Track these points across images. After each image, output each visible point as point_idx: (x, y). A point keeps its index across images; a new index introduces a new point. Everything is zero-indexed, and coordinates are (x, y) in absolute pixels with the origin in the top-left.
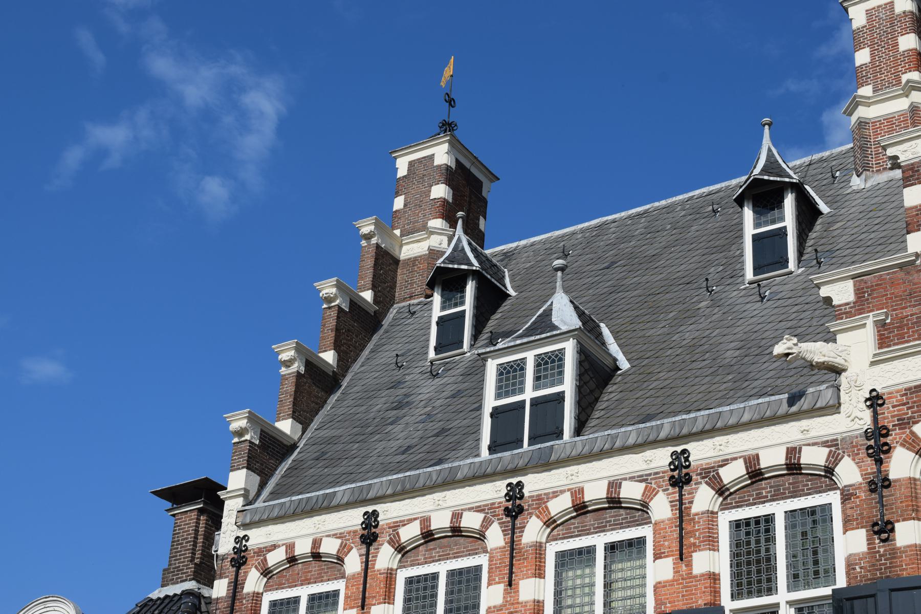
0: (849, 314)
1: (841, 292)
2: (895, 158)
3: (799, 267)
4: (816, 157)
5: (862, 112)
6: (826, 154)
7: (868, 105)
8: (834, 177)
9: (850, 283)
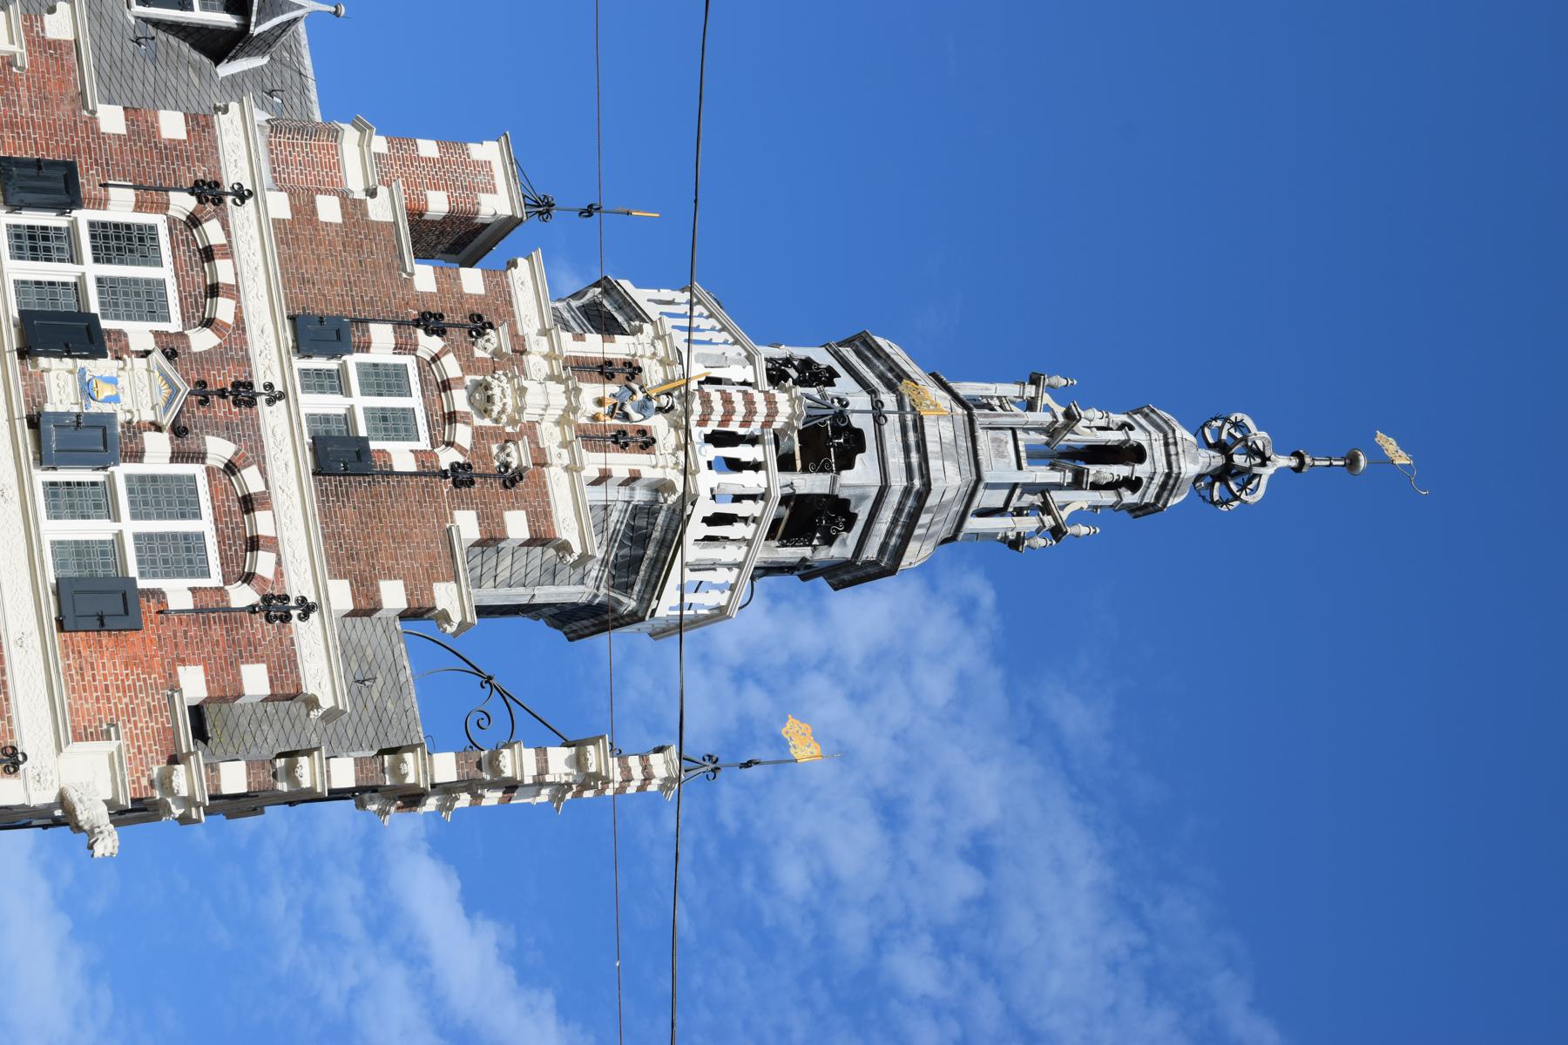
0: (28, 30)
1: (59, 26)
2: (226, 110)
3: (137, 17)
4: (312, 84)
5: (350, 135)
6: (313, 95)
7: (360, 145)
8: (270, 93)
9: (70, 37)
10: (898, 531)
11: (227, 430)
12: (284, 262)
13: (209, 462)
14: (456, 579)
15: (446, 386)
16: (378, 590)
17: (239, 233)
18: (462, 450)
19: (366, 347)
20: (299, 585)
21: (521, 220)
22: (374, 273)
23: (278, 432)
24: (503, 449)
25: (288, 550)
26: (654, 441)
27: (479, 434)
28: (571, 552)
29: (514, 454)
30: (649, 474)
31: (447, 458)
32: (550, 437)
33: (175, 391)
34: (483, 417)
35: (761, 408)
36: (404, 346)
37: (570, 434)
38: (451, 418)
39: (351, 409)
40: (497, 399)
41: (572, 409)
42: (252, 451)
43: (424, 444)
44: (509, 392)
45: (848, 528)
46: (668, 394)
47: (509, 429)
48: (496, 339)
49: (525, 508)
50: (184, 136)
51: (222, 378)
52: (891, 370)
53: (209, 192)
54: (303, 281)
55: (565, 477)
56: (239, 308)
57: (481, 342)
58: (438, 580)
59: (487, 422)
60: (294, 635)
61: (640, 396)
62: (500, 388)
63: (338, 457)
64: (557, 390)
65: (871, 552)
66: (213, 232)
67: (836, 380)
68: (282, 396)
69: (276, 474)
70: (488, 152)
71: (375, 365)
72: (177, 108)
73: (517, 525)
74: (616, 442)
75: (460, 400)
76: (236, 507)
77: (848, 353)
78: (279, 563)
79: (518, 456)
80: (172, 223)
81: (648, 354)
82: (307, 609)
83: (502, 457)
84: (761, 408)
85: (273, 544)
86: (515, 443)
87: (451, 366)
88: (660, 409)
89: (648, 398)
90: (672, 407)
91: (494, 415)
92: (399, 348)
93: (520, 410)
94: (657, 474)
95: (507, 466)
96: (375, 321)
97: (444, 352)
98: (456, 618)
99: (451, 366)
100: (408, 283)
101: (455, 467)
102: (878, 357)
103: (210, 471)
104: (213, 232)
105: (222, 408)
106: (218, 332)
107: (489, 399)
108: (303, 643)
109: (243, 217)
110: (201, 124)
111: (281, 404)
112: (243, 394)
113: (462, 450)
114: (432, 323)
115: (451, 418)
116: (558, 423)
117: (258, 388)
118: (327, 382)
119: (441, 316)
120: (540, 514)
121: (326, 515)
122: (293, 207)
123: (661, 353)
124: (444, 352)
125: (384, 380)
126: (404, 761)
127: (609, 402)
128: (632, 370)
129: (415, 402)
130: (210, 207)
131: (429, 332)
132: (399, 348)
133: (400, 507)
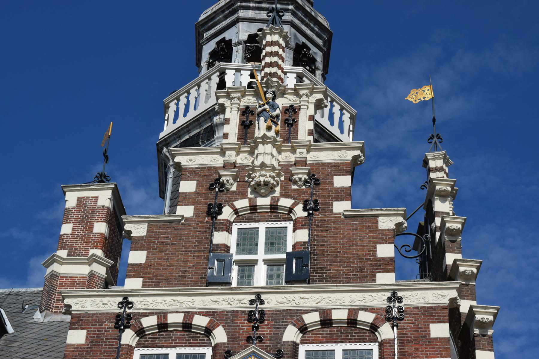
2: (69, 306)
4: (15, 290)
6: (23, 290)
7: (62, 264)
8: (23, 308)
10: (312, 25)
11: (280, 328)
12: (169, 283)
13: (298, 341)
14: (377, 216)
15: (253, 208)
16: (383, 258)
17: (151, 307)
18: (295, 204)
19: (227, 248)
20: (380, 300)
21: (116, 185)
22: (180, 237)
23: (280, 300)
24: (295, 182)
25: (357, 303)
26: (292, 106)
27: (285, 194)
28: (359, 156)
29: (300, 176)
30: (311, 111)
31: (299, 212)
32: (287, 157)
33: (253, 354)
34: (275, 191)
35: (275, 49)
36: (227, 227)
37: (288, 146)
38: (274, 207)
39: (266, 261)
40: (267, 179)
41: (274, 143)
42: (294, 316)
43: (290, 225)
44: (263, 173)
45: (309, 49)
46: (265, 93)
47: (283, 178)
48: (227, 177)
49: (332, 176)
50: (84, 332)
51: (245, 328)
52: (223, 11)
53: (122, 321)
54: (184, 276)
55: (312, 153)
56: (200, 313)
57: (228, 186)
58: (377, 226)
59: (278, 189)
60: (412, 306)
61: (266, 107)
62: (260, 177)
63: (300, 269)
64: (261, 148)
65: (320, 42)
66: (149, 322)
67: (227, 39)
68: (258, 295)
69: (308, 304)
70: (72, 198)
71: (238, 245)
72: (66, 333)
73: (342, 181)
74: (292, 125)
75: (264, 202)
76: (328, 330)
77: (207, 35)
78: (365, 310)
79: (301, 174)
80: (139, 345)
81: (238, 102)
82: (394, 298)
83: (300, 183)
84: (275, 49)
85: (353, 312)
86: (293, 175)
87: (242, 204)
88: (274, 99)
89: (268, 103)
90: (274, 92)
91: (275, 183)
92: (229, 230)
93: (274, 169)
94: (312, 107)
95: (306, 181)
96: (211, 241)
97: (232, 206)
98: (400, 219)
99: (242, 204)
100: (188, 220)
101: (305, 209)
102: (214, 18)
103: (303, 342)
104: (149, 322)
105: (265, 330)
106: (215, 327)
107: (266, 184)
108: (416, 302)
109: (139, 304)
110: (78, 321)
111: (263, 297)
112: (256, 318)
113: (295, 204)
114: (214, 211)
115: (274, 207)
116: (280, 153)
117: (253, 308)
118: (247, 273)
119: (210, 205)
120: (337, 168)
121: (335, 280)
122: (134, 276)
123: (239, 95)
124: (232, 206)
125: (248, 241)
126: (464, 272)
127: (270, 123)
128: (246, 112)
129: (262, 227)
130: (133, 322)
131: (220, 213)
132: (229, 230)
133: (331, 241)
